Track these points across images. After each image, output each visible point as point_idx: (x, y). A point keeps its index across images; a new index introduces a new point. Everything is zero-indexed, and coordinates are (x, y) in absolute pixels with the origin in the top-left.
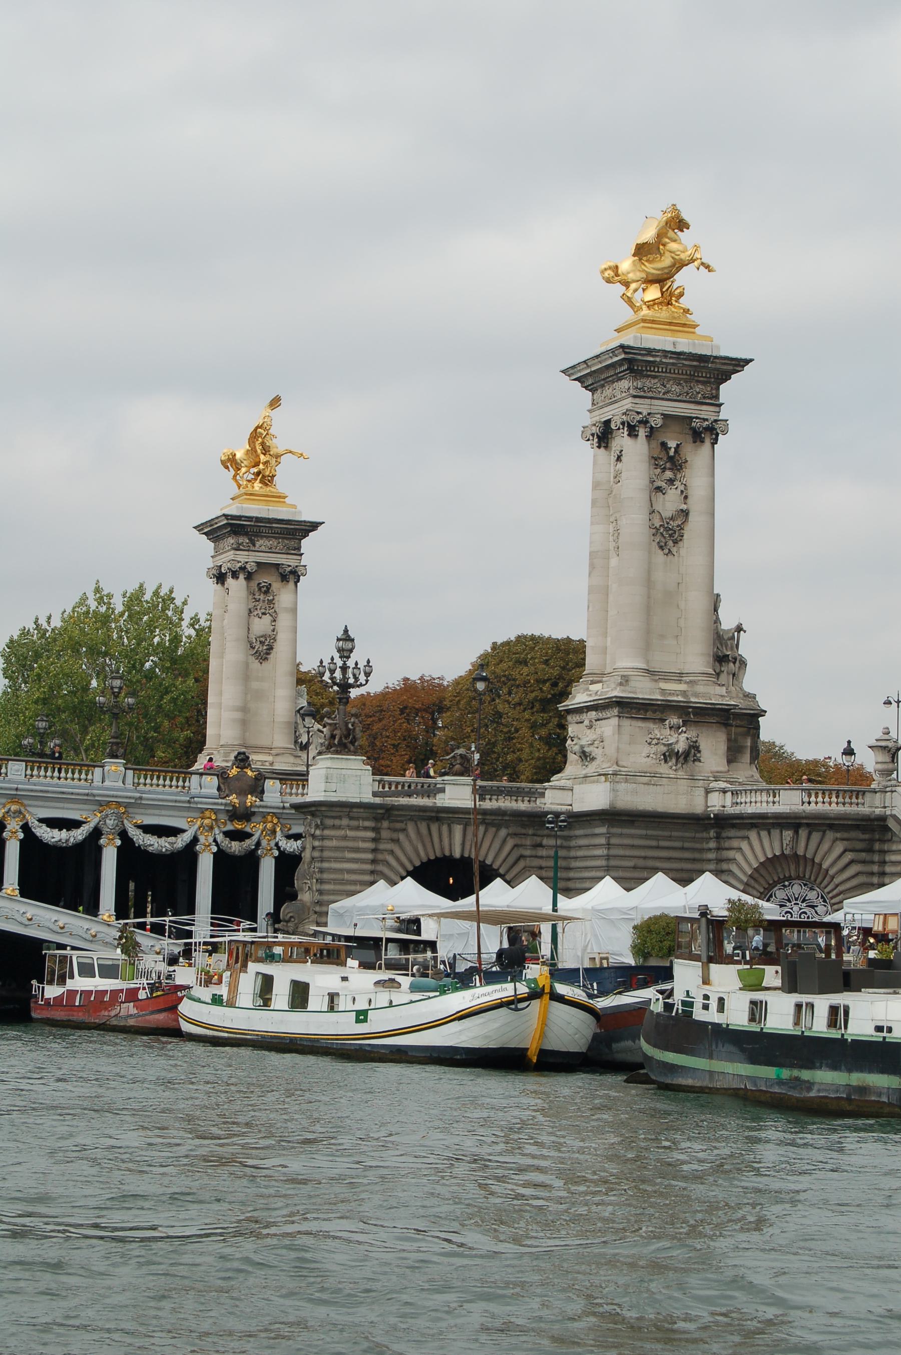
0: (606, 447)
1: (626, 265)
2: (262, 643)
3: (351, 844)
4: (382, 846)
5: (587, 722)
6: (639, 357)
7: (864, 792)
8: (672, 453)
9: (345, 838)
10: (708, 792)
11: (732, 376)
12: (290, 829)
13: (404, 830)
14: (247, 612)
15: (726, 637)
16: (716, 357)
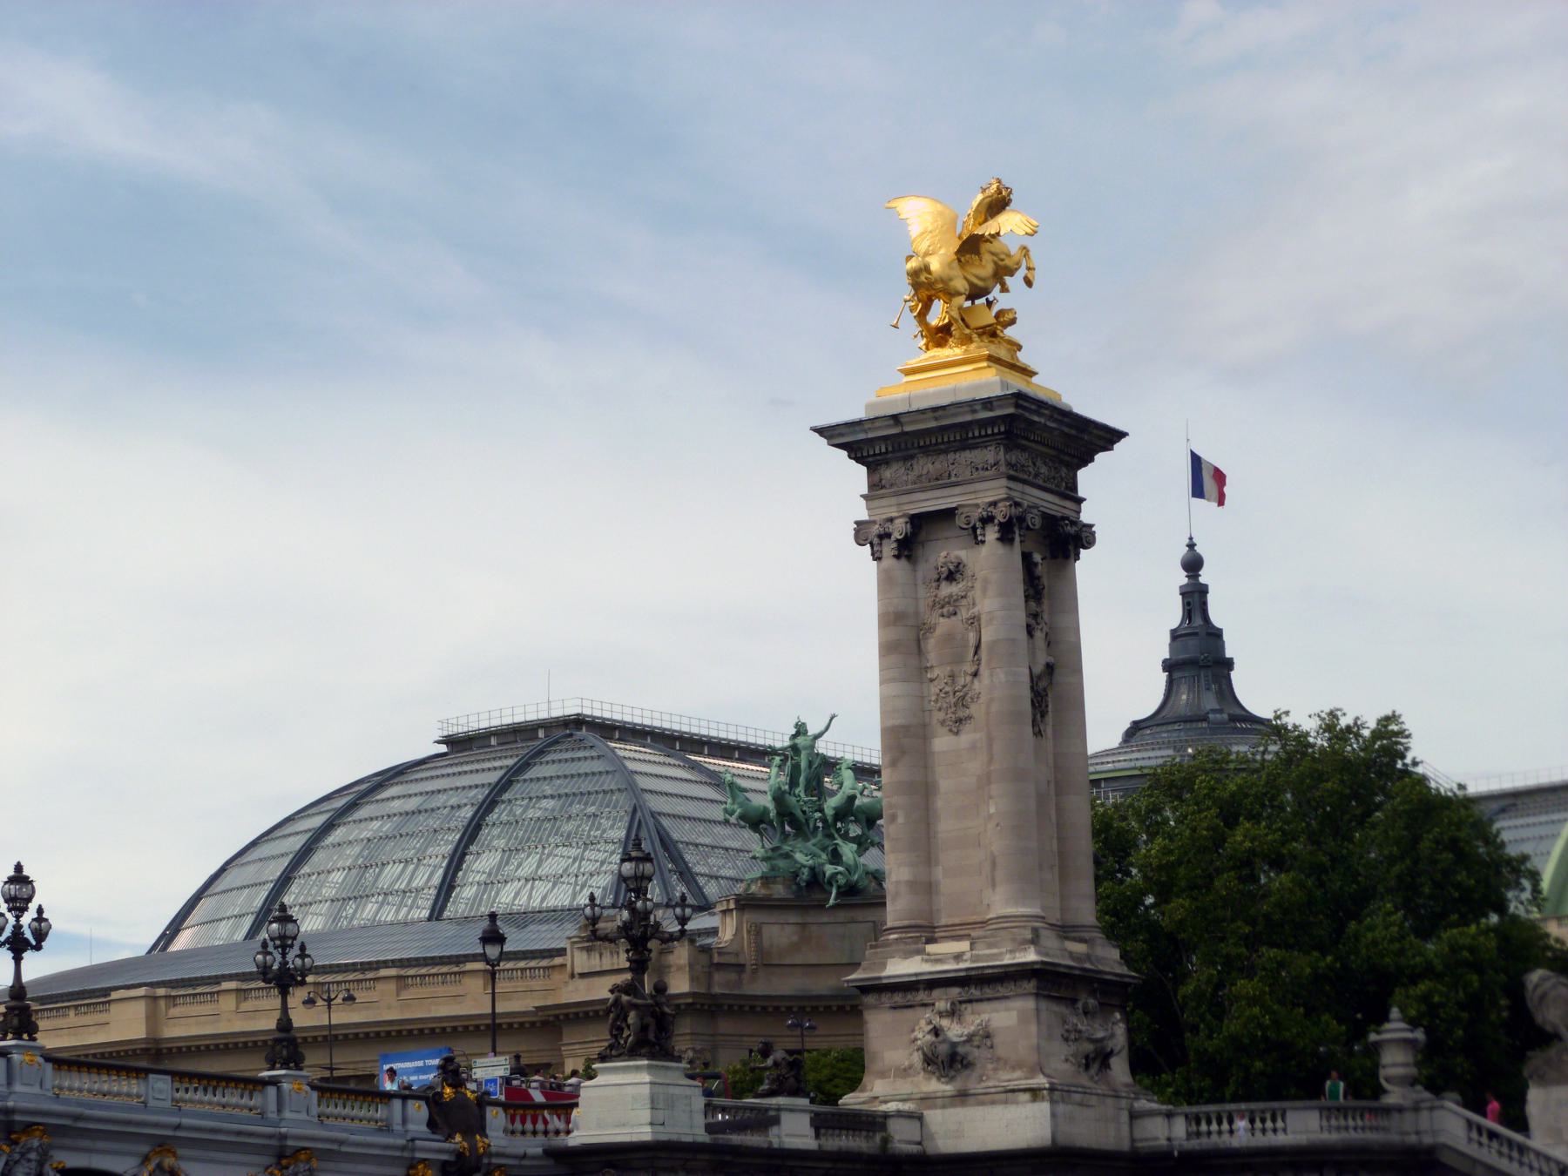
0: (909, 558)
6: (1027, 414)
10: (1134, 1116)
11: (1099, 457)
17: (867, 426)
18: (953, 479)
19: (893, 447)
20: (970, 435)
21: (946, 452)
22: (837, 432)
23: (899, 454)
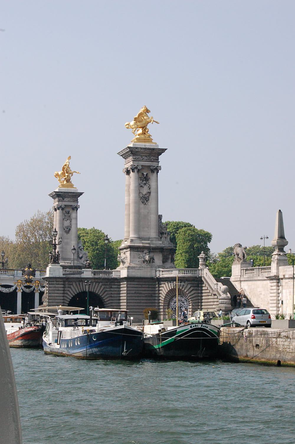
1: (132, 123)
2: (67, 228)
3: (56, 289)
4: (66, 289)
5: (123, 253)
6: (134, 150)
7: (196, 270)
8: (145, 176)
9: (55, 287)
12: (43, 285)
13: (72, 284)
14: (63, 219)
15: (163, 227)
16: (156, 149)
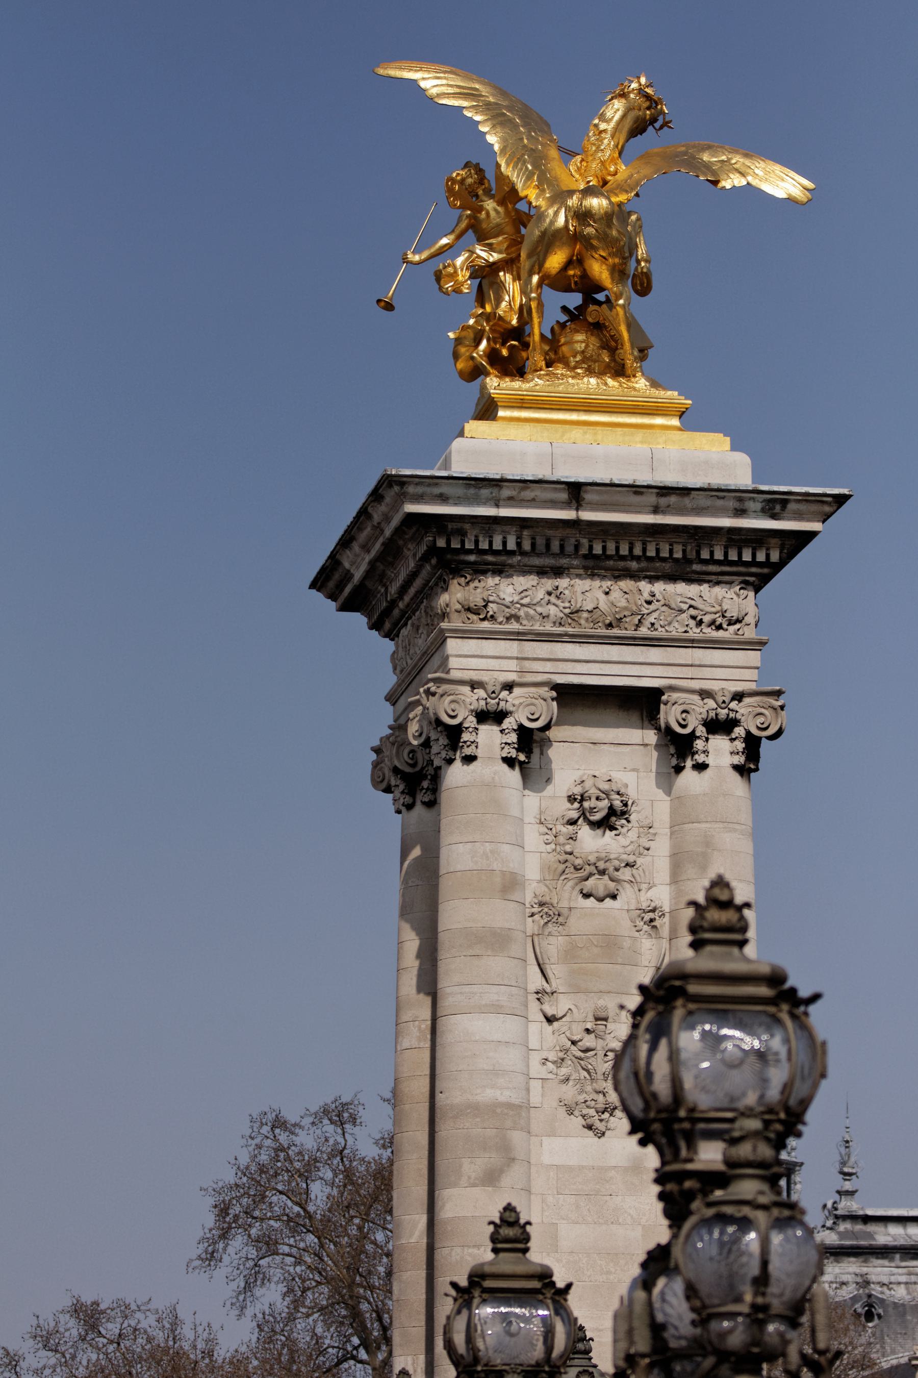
17: (506, 492)
18: (644, 631)
19: (533, 545)
20: (705, 555)
21: (634, 576)
22: (437, 491)
23: (536, 561)
